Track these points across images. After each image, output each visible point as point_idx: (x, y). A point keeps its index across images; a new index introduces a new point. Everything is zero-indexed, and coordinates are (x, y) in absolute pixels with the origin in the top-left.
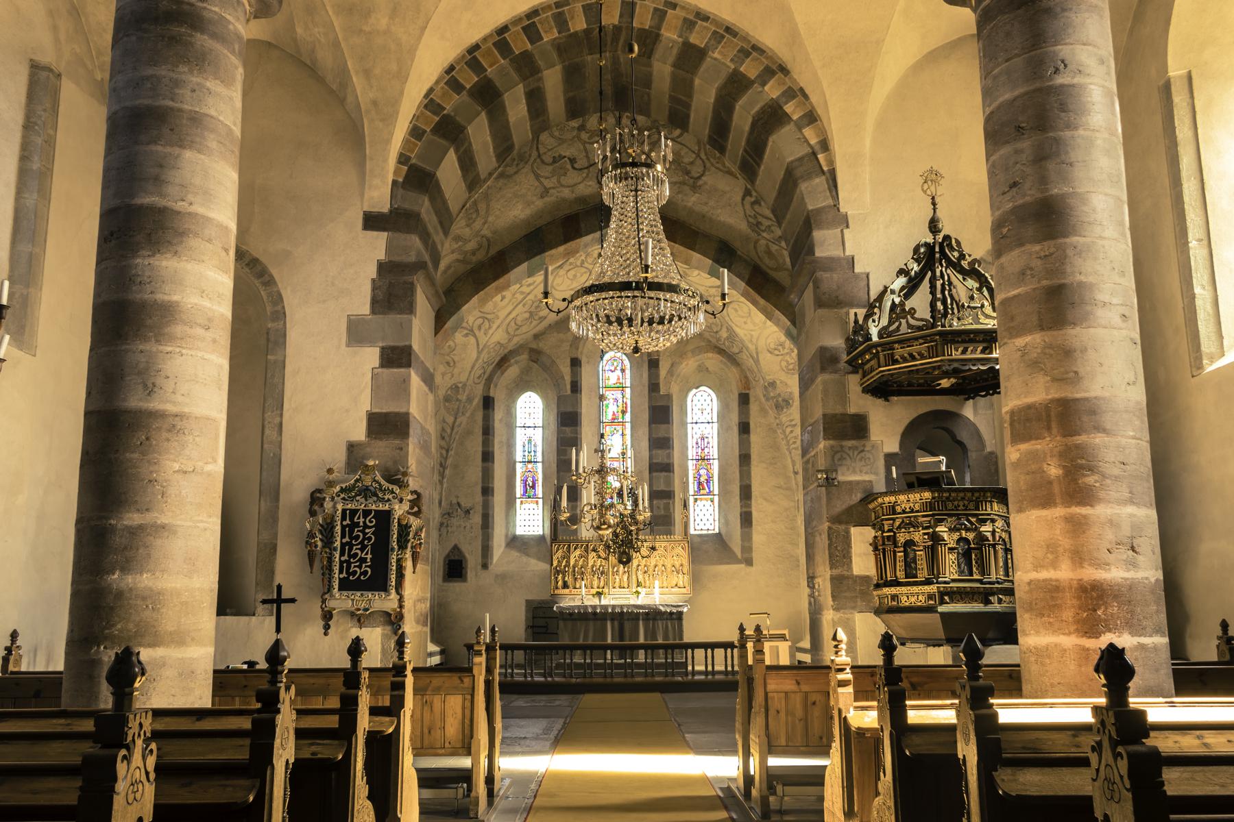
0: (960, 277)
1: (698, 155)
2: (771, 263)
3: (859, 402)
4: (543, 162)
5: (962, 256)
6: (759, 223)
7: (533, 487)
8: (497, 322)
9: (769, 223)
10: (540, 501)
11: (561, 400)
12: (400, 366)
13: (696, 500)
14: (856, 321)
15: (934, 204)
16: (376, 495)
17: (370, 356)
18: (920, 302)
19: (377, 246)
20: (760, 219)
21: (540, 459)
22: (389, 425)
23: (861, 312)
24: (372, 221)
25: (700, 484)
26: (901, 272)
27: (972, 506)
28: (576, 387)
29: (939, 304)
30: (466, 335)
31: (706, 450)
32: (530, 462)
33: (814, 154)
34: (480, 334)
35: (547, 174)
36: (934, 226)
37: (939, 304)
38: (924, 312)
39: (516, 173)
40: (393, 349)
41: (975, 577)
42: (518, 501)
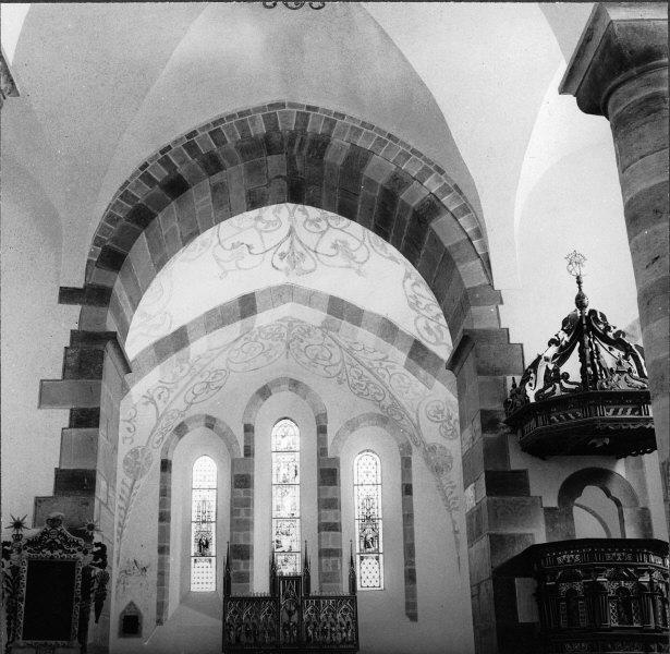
0: (606, 346)
1: (362, 243)
3: (517, 461)
5: (608, 328)
7: (207, 546)
8: (176, 391)
10: (214, 559)
11: (234, 463)
12: (88, 426)
13: (362, 559)
14: (514, 386)
15: (579, 283)
16: (62, 548)
17: (61, 417)
18: (573, 367)
19: (71, 316)
20: (420, 299)
21: (213, 519)
22: (76, 482)
23: (518, 379)
24: (67, 295)
25: (367, 544)
26: (552, 342)
27: (629, 557)
28: (249, 452)
29: (589, 369)
31: (372, 511)
32: (204, 522)
33: (470, 240)
34: (160, 404)
36: (580, 301)
37: (589, 369)
38: (575, 376)
40: (83, 411)
41: (635, 625)
42: (193, 559)
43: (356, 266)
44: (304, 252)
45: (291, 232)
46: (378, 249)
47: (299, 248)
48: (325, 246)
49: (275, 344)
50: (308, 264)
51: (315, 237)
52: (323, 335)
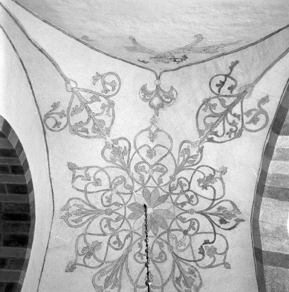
1: (196, 170)
2: (262, 117)
4: (200, 260)
6: (231, 130)
9: (226, 124)
35: (212, 259)
39: (201, 279)
43: (218, 175)
44: (217, 206)
45: (201, 213)
46: (197, 160)
47: (214, 210)
48: (208, 193)
50: (228, 206)
51: (200, 199)
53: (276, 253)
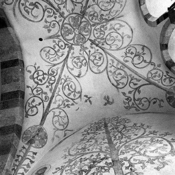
30: (139, 92)
34: (140, 84)
49: (108, 28)
52: (89, 7)
53: (9, 61)
